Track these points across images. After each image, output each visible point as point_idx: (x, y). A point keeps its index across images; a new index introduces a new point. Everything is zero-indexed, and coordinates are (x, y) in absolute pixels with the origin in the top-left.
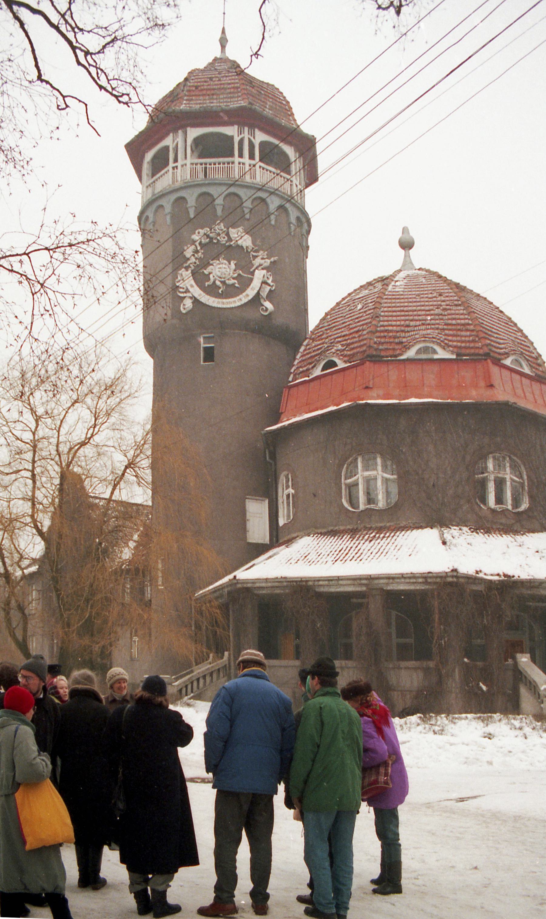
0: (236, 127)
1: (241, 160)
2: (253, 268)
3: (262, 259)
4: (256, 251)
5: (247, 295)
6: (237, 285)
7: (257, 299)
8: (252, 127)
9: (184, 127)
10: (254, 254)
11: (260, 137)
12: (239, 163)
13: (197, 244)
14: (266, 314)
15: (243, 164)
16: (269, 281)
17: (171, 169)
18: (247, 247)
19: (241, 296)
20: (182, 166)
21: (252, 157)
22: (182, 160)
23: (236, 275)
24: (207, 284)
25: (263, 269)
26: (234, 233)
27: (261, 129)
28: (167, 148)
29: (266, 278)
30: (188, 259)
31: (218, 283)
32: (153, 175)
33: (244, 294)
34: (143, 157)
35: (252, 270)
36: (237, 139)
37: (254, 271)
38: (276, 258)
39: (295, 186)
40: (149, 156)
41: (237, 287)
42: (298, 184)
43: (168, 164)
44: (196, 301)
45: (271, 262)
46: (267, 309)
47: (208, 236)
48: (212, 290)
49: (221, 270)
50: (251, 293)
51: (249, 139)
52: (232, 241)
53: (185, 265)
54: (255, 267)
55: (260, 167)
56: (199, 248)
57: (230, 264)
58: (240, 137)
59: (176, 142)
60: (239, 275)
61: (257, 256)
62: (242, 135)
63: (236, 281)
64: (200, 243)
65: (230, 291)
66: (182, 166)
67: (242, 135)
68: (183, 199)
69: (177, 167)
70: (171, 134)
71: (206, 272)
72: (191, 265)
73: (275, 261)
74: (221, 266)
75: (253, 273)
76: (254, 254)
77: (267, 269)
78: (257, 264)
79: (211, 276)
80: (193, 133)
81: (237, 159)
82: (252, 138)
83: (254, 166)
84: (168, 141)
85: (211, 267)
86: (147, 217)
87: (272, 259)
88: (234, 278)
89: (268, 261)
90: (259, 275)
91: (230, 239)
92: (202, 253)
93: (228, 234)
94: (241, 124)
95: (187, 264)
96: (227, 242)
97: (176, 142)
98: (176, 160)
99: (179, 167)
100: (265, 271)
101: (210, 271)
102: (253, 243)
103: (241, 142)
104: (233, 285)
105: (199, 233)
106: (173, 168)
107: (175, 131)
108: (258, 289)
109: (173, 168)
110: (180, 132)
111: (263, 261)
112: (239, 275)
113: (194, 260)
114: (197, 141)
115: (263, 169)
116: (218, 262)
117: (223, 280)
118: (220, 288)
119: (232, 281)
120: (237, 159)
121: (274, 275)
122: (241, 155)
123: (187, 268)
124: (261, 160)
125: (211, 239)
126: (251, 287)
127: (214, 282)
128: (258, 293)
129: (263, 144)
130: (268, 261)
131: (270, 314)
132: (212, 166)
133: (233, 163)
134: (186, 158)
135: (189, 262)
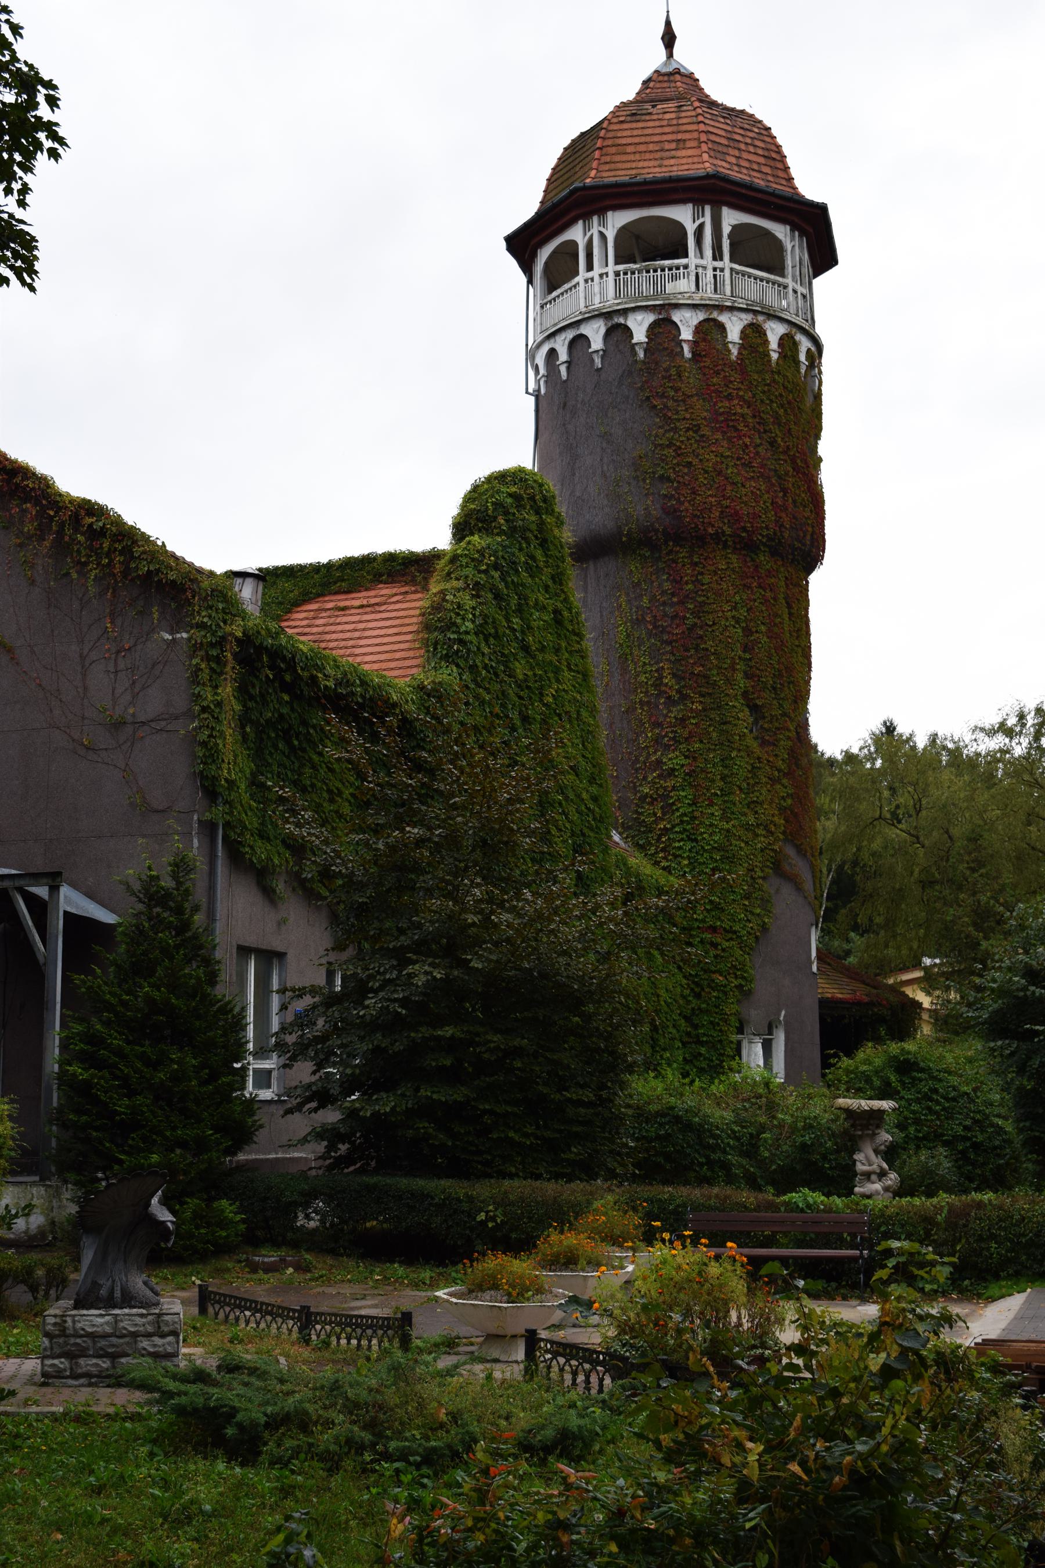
0: (691, 205)
9: (602, 212)
11: (731, 218)
15: (705, 268)
20: (601, 276)
21: (717, 255)
22: (601, 267)
32: (550, 292)
34: (533, 256)
36: (691, 229)
40: (544, 254)
55: (732, 269)
58: (698, 223)
59: (588, 235)
62: (701, 220)
66: (601, 276)
67: (701, 220)
69: (592, 280)
70: (581, 222)
81: (692, 260)
83: (722, 270)
84: (576, 234)
97: (588, 235)
98: (590, 267)
107: (586, 217)
109: (586, 281)
110: (595, 219)
114: (623, 233)
124: (732, 260)
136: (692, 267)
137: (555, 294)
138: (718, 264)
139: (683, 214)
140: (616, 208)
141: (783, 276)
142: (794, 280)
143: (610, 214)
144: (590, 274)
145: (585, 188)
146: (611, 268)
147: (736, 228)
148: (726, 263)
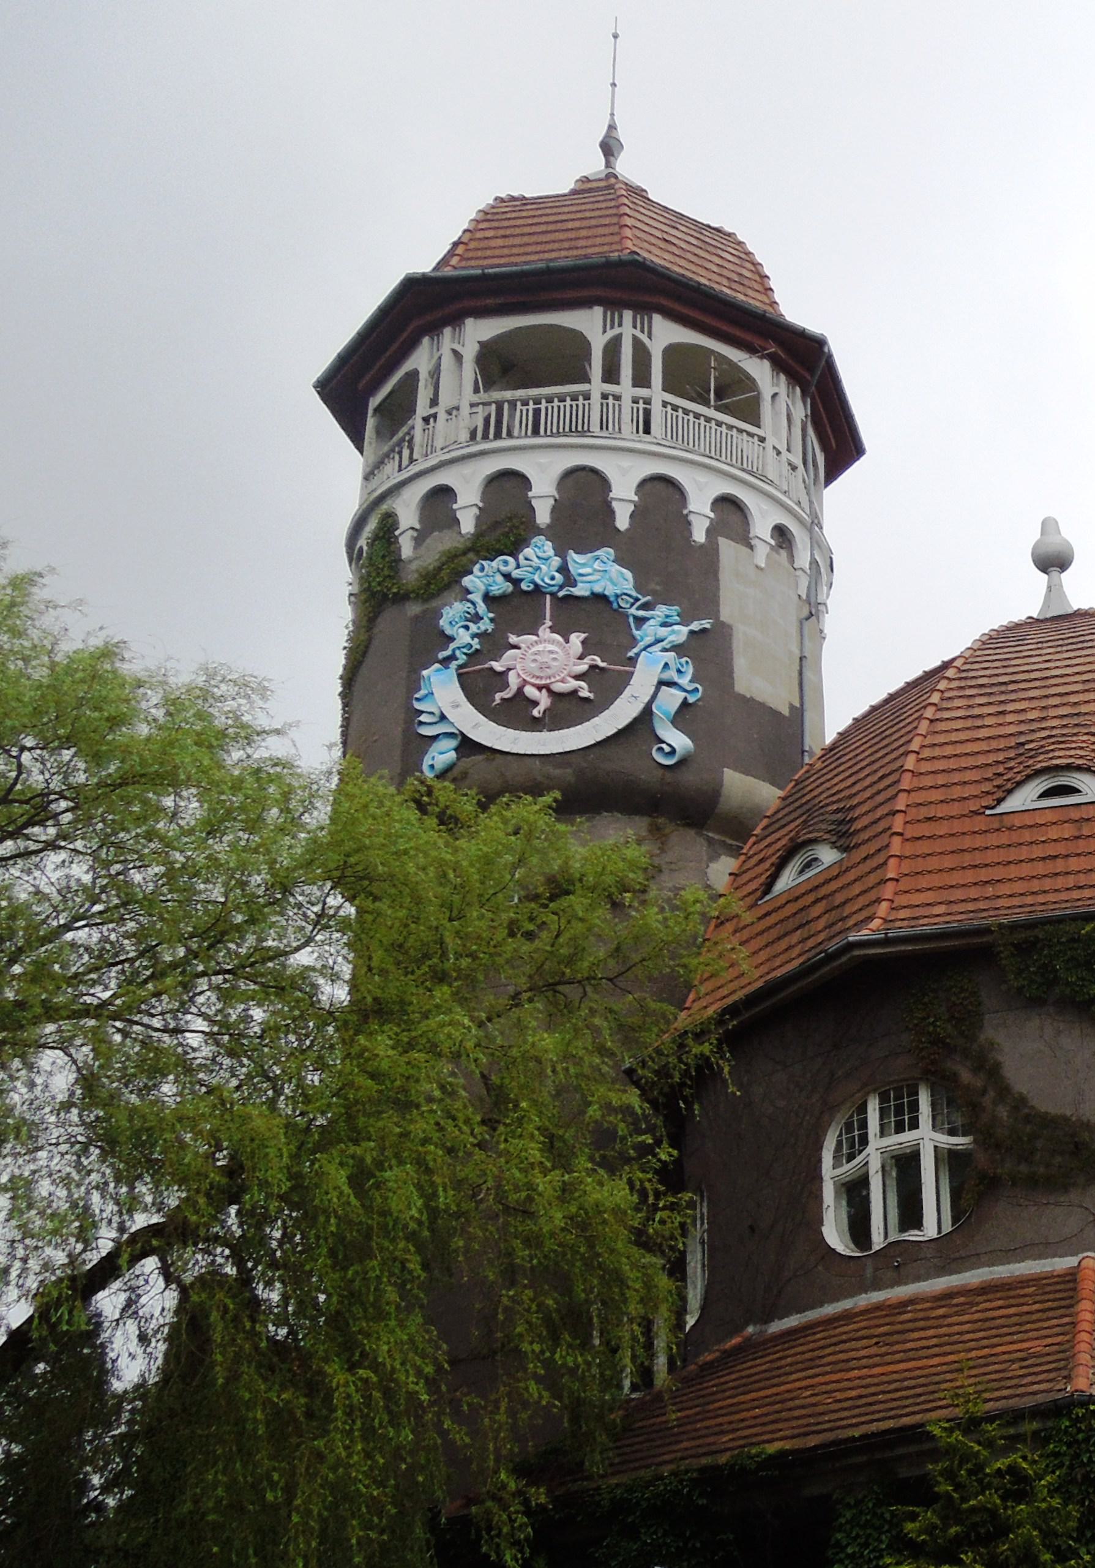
0: (598, 311)
2: (635, 650)
3: (664, 625)
4: (646, 606)
6: (585, 693)
8: (643, 309)
10: (641, 613)
11: (665, 333)
12: (605, 396)
13: (477, 597)
15: (617, 398)
16: (684, 681)
18: (617, 596)
21: (641, 379)
23: (583, 667)
24: (498, 696)
25: (665, 650)
27: (671, 315)
30: (452, 639)
31: (530, 692)
35: (631, 654)
36: (598, 343)
37: (638, 655)
38: (706, 624)
39: (771, 453)
41: (586, 699)
42: (783, 448)
44: (467, 746)
47: (507, 577)
48: (516, 712)
49: (546, 658)
51: (635, 338)
52: (574, 584)
53: (442, 655)
54: (641, 645)
55: (665, 404)
56: (482, 608)
57: (567, 641)
58: (610, 334)
60: (593, 667)
61: (648, 619)
62: (617, 331)
63: (583, 684)
64: (488, 598)
65: (568, 709)
67: (617, 331)
71: (498, 666)
72: (458, 653)
73: (704, 631)
74: (540, 647)
75: (633, 661)
76: (641, 613)
77: (678, 649)
78: (649, 640)
81: (597, 386)
82: (644, 338)
87: (695, 626)
88: (577, 677)
89: (685, 630)
91: (570, 581)
92: (492, 620)
93: (564, 569)
94: (613, 306)
95: (448, 653)
96: (561, 587)
101: (510, 663)
102: (637, 588)
103: (613, 349)
104: (574, 692)
105: (482, 569)
108: (647, 699)
111: (663, 632)
112: (593, 667)
113: (468, 640)
115: (675, 408)
117: (543, 682)
118: (535, 704)
119: (573, 684)
120: (597, 386)
122: (611, 374)
123: (446, 662)
125: (516, 582)
127: (520, 691)
128: (647, 714)
130: (685, 630)
131: (682, 762)
133: (587, 397)
135: (452, 646)
136: (596, 397)
139: (590, 324)
142: (776, 433)
147: (672, 352)
148: (657, 392)
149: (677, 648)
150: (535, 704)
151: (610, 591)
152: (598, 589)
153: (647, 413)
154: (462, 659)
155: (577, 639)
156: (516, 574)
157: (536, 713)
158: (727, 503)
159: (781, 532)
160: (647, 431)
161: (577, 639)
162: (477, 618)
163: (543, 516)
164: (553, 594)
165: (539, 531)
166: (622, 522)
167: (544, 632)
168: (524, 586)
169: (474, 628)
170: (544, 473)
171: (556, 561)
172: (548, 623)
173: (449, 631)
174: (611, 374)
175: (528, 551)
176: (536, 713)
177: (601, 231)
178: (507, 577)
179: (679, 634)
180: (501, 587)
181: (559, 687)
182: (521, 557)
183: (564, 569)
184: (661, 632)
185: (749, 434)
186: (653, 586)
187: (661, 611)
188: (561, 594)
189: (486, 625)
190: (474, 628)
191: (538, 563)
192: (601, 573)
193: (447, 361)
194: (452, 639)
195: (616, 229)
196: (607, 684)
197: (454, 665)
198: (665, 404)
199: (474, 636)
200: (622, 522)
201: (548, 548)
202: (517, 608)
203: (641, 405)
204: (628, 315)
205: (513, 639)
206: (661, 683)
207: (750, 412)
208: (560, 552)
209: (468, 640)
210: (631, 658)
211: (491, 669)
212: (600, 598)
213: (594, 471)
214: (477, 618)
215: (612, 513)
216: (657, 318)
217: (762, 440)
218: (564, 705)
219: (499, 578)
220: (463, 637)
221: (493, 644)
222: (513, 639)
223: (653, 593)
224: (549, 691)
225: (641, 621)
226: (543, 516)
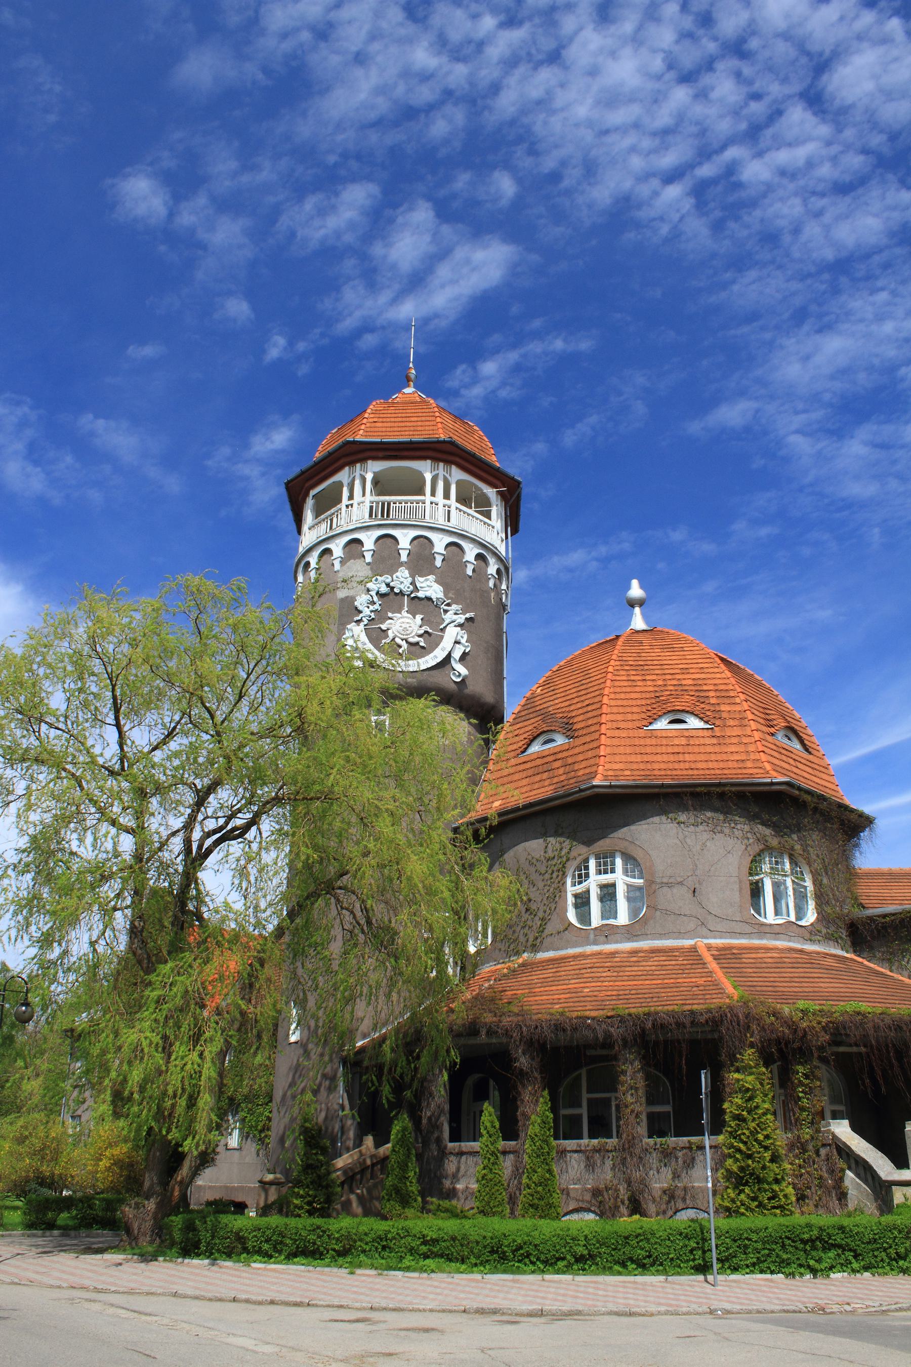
0: (429, 462)
1: (433, 499)
2: (444, 625)
3: (456, 614)
4: (448, 605)
5: (436, 657)
6: (422, 644)
7: (446, 661)
8: (449, 462)
9: (363, 460)
10: (446, 608)
11: (457, 474)
12: (431, 503)
13: (373, 593)
14: (459, 680)
16: (463, 641)
17: (344, 508)
19: (427, 658)
21: (447, 496)
24: (383, 641)
26: (420, 581)
28: (340, 485)
29: (459, 637)
30: (360, 612)
31: (398, 640)
33: (432, 655)
35: (442, 627)
36: (428, 477)
37: (445, 627)
38: (472, 615)
41: (423, 647)
43: (340, 501)
45: (466, 619)
46: (460, 675)
50: (439, 655)
53: (356, 618)
55: (457, 508)
56: (375, 599)
58: (434, 473)
60: (426, 632)
62: (436, 472)
63: (421, 639)
64: (377, 593)
67: (436, 472)
68: (358, 542)
69: (352, 505)
70: (347, 468)
71: (384, 627)
73: (471, 618)
75: (443, 630)
76: (446, 608)
77: (460, 625)
79: (390, 632)
80: (373, 468)
81: (428, 498)
82: (448, 476)
84: (343, 476)
85: (390, 621)
86: (308, 564)
87: (468, 615)
88: (420, 636)
89: (464, 617)
90: (452, 633)
91: (416, 589)
95: (359, 618)
96: (412, 593)
97: (352, 476)
98: (351, 497)
99: (355, 506)
100: (459, 629)
102: (445, 595)
104: (417, 643)
105: (376, 580)
106: (347, 506)
107: (352, 463)
109: (347, 506)
110: (358, 465)
111: (455, 617)
112: (426, 632)
113: (369, 613)
115: (460, 510)
116: (398, 615)
119: (417, 639)
121: (469, 633)
122: (433, 494)
125: (392, 588)
126: (440, 647)
127: (393, 639)
128: (449, 656)
129: (459, 483)
132: (398, 505)
134: (364, 495)
135: (361, 615)
137: (322, 517)
138: (447, 502)
140: (375, 458)
141: (490, 519)
143: (370, 462)
144: (351, 502)
145: (354, 442)
146: (369, 498)
149: (460, 625)
150: (400, 647)
151: (434, 597)
152: (428, 594)
153: (449, 511)
154: (366, 622)
155: (419, 617)
156: (392, 584)
157: (401, 651)
158: (479, 557)
159: (498, 571)
160: (449, 521)
161: (419, 617)
162: (373, 603)
163: (404, 557)
164: (408, 596)
165: (401, 564)
166: (438, 562)
167: (404, 613)
168: (396, 590)
169: (371, 608)
170: (404, 538)
171: (410, 580)
172: (406, 609)
173: (360, 608)
174: (433, 494)
175: (398, 574)
176: (401, 651)
177: (427, 423)
178: (388, 585)
179: (461, 619)
180: (384, 589)
181: (411, 640)
182: (394, 576)
183: (413, 583)
184: (454, 615)
185: (489, 525)
186: (450, 595)
187: (454, 607)
188: (412, 595)
189: (377, 607)
190: (371, 608)
191: (402, 579)
192: (430, 588)
193: (357, 474)
194: (360, 612)
195: (434, 423)
196: (432, 639)
197: (362, 624)
198: (457, 508)
199: (372, 611)
200: (438, 562)
201: (407, 572)
202: (391, 599)
203: (447, 508)
204: (441, 465)
205: (390, 615)
206: (457, 642)
207: (488, 515)
208: (412, 576)
209: (369, 613)
210: (442, 630)
211: (380, 628)
212: (429, 599)
213: (426, 538)
214: (373, 603)
215: (435, 558)
216: (454, 467)
217: (493, 527)
218: (413, 648)
219: (384, 585)
220: (366, 612)
221: (381, 616)
222: (390, 615)
223: (451, 598)
224: (407, 642)
225: (446, 611)
226: (404, 557)
